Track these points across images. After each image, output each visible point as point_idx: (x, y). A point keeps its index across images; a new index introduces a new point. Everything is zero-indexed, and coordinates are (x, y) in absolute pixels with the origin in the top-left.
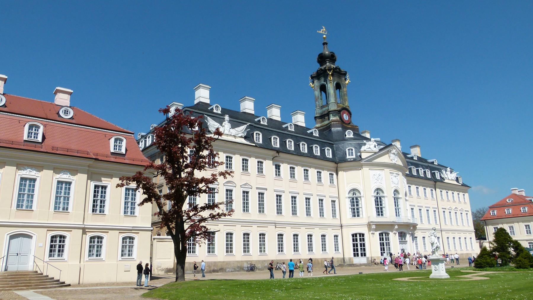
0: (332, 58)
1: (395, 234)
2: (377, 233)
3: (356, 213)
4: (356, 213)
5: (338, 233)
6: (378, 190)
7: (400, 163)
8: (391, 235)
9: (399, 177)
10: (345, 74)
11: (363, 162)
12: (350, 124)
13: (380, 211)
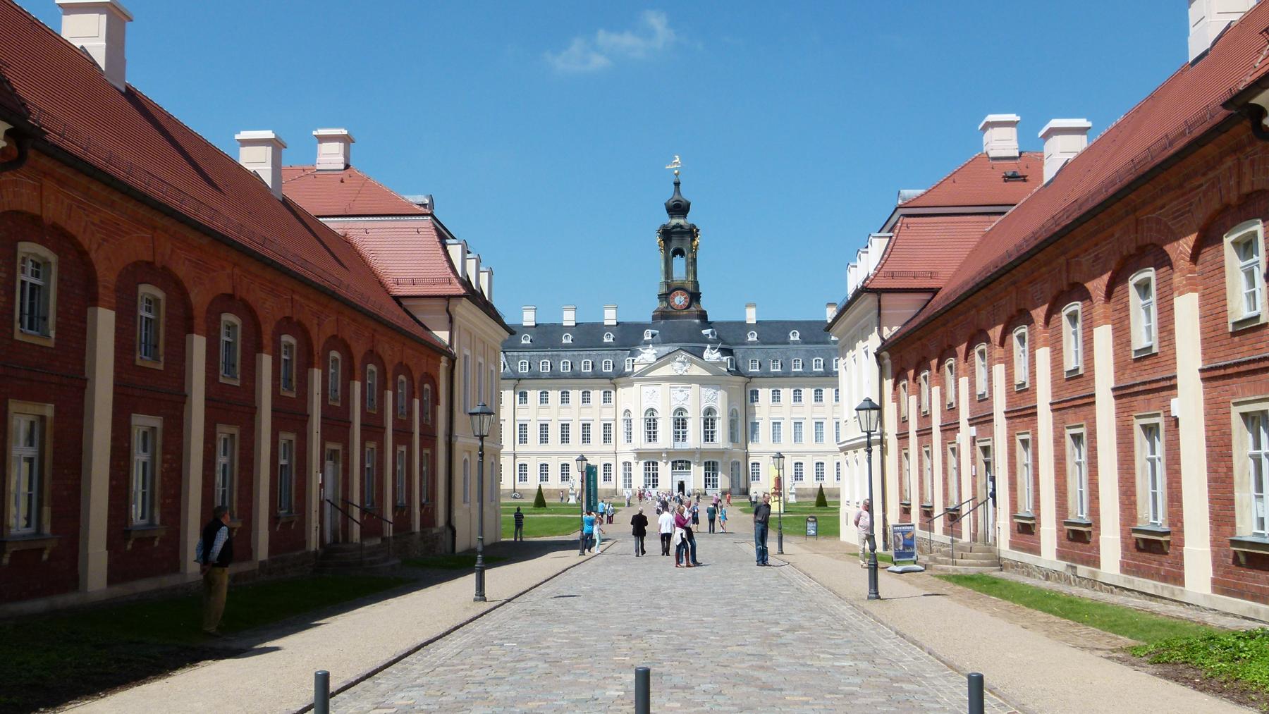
0: (678, 208)
2: (642, 463)
3: (629, 439)
4: (629, 439)
5: (611, 461)
6: (652, 411)
7: (696, 371)
8: (661, 465)
9: (689, 392)
10: (692, 233)
11: (632, 377)
12: (688, 307)
13: (652, 436)
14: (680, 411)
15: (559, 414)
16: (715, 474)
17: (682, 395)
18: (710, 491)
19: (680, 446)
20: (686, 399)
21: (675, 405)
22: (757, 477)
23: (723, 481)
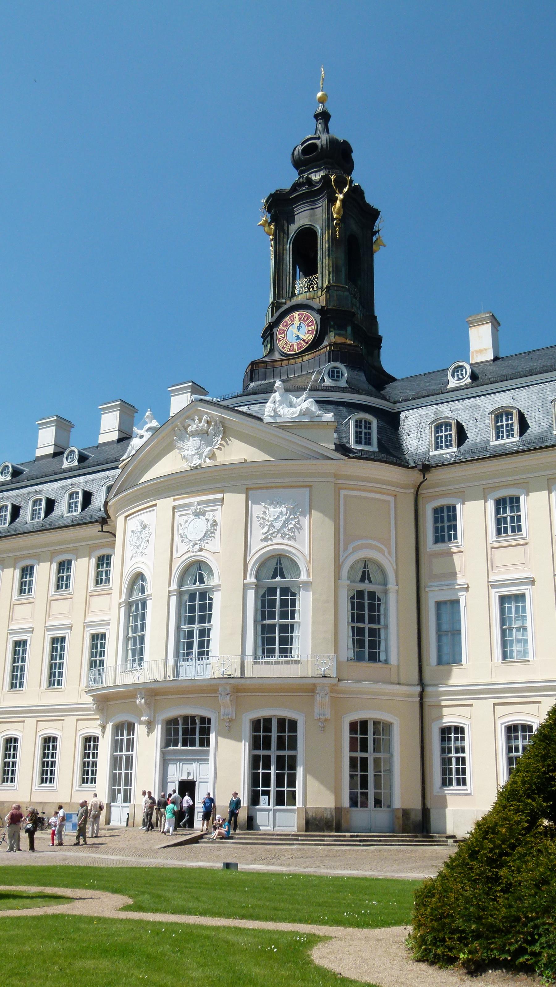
1: (150, 726)
2: (109, 727)
7: (237, 452)
8: (140, 730)
9: (218, 514)
14: (197, 570)
15: (11, 618)
16: (288, 766)
17: (199, 526)
18: (269, 817)
19: (193, 671)
20: (209, 534)
21: (183, 554)
22: (454, 771)
23: (316, 791)
